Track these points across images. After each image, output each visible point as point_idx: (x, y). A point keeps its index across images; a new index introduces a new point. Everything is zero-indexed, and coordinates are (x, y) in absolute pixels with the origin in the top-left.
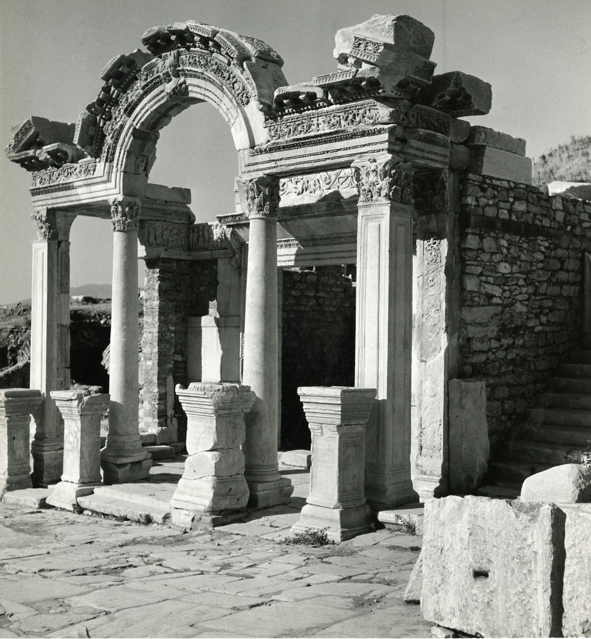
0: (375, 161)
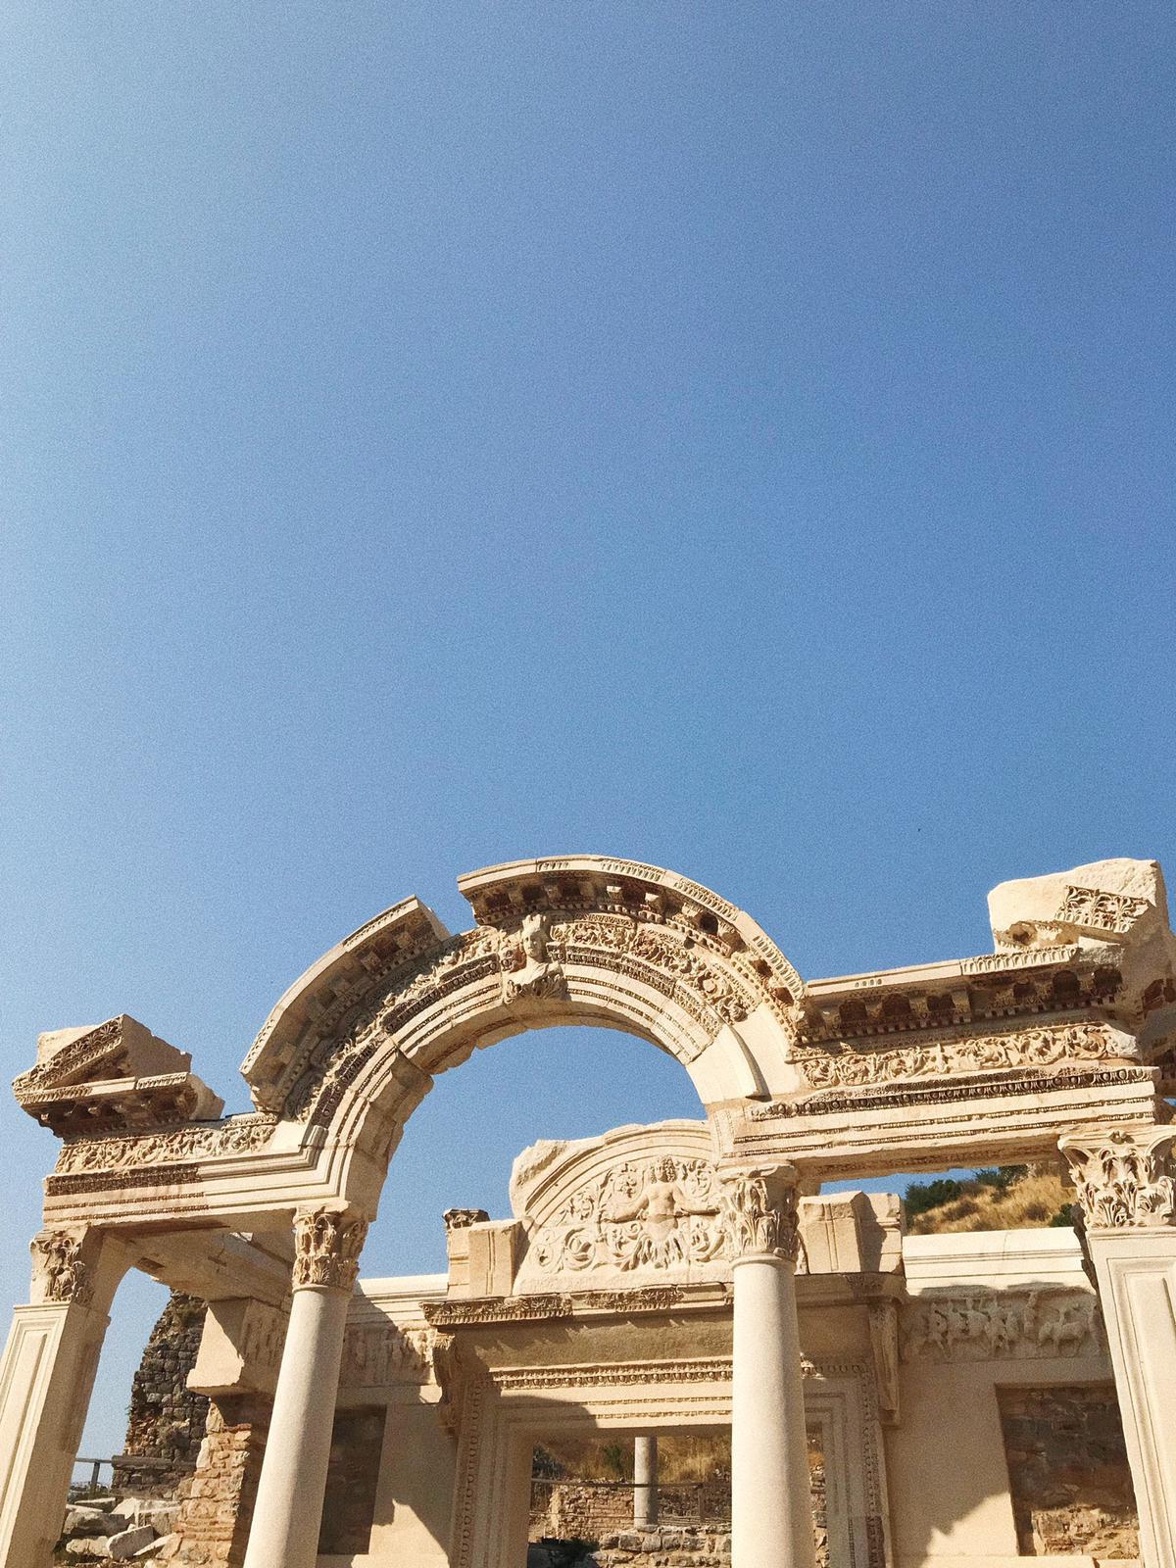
0: (1128, 1139)
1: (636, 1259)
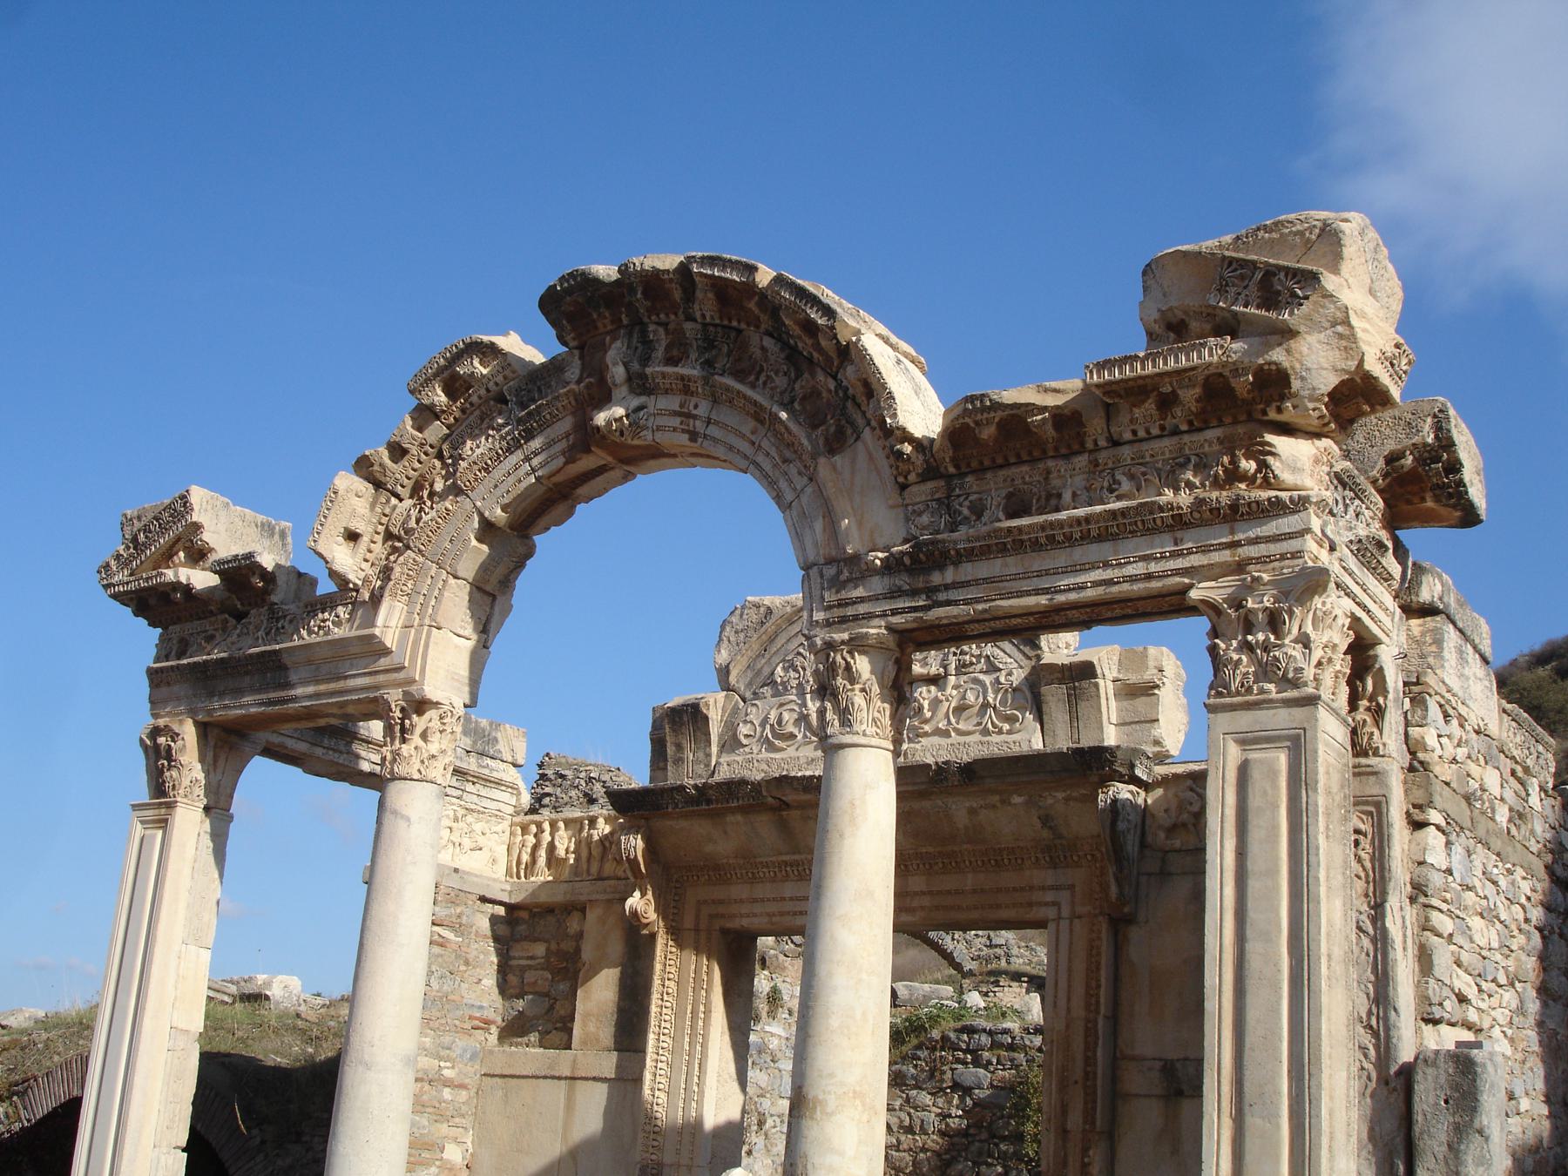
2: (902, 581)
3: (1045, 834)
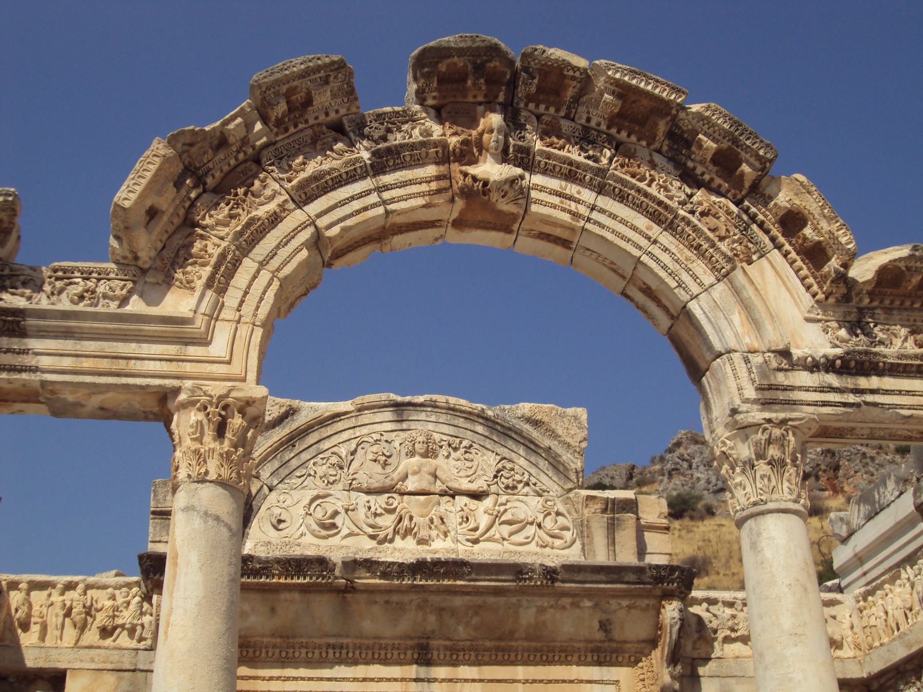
1: (396, 532)
2: (832, 379)
3: (600, 635)
